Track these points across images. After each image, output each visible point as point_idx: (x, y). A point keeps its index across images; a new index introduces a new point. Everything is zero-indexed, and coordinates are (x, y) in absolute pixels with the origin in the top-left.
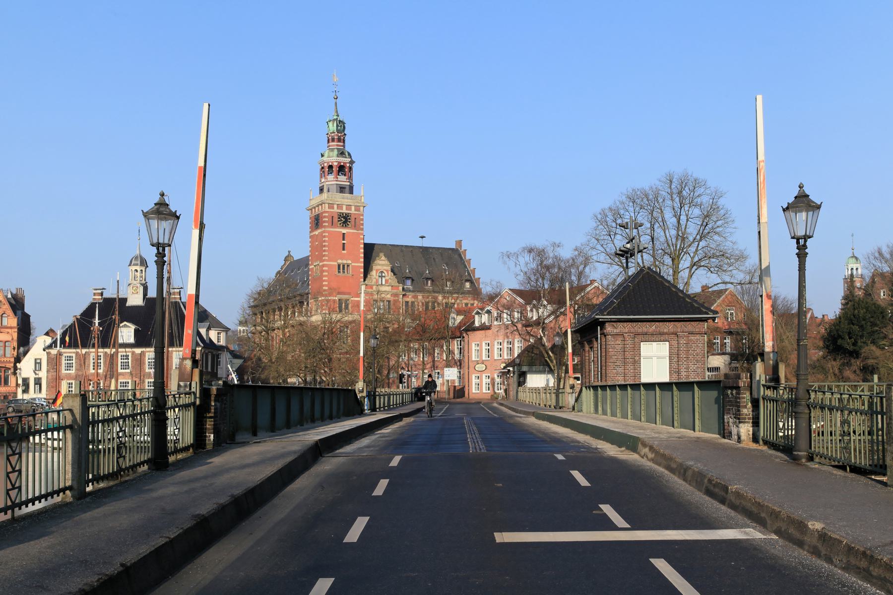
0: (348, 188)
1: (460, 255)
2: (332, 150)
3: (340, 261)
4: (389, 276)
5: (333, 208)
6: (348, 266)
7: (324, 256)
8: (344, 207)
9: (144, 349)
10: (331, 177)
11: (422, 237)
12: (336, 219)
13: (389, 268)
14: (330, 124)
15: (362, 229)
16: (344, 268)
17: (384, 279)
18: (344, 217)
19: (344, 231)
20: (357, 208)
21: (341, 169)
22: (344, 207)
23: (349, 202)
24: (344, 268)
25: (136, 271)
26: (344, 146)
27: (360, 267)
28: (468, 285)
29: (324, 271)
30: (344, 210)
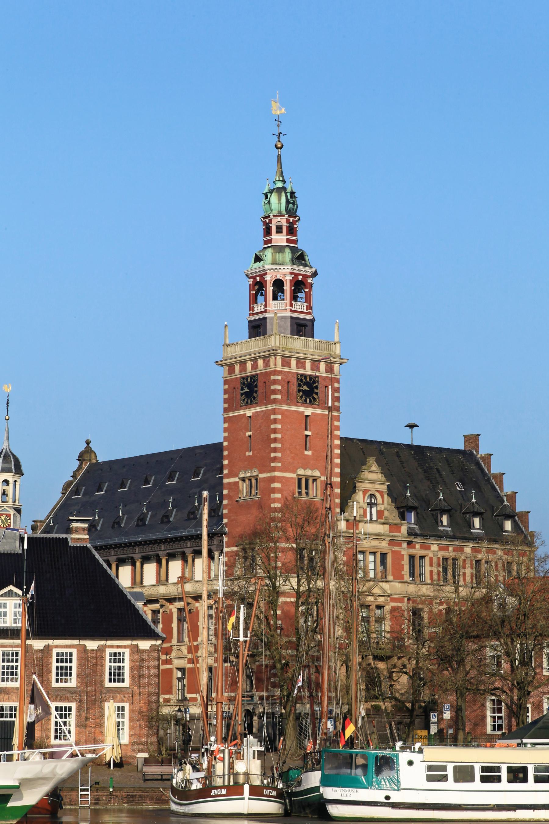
1: (478, 464)
3: (301, 472)
4: (384, 502)
7: (275, 459)
8: (308, 364)
9: (50, 642)
11: (412, 426)
12: (294, 388)
13: (384, 488)
14: (274, 198)
17: (374, 510)
18: (308, 384)
20: (330, 369)
22: (308, 364)
25: (6, 482)
28: (508, 525)
29: (274, 490)
30: (308, 370)
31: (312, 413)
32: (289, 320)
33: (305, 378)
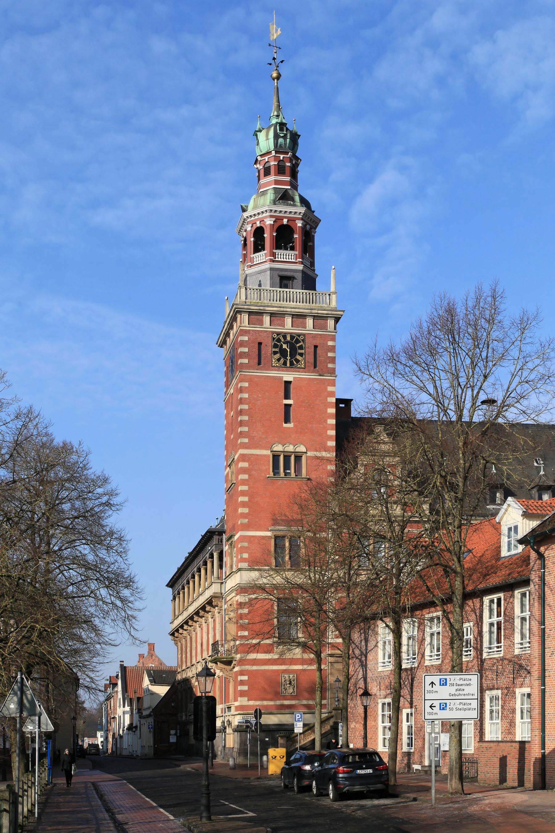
0: (299, 276)
2: (264, 193)
3: (278, 448)
5: (261, 323)
6: (298, 458)
10: (261, 257)
12: (268, 349)
14: (262, 136)
15: (332, 372)
16: (287, 466)
19: (288, 376)
21: (283, 236)
23: (301, 307)
24: (287, 466)
26: (295, 187)
27: (328, 460)
31: (294, 378)
32: (269, 272)
33: (285, 337)
